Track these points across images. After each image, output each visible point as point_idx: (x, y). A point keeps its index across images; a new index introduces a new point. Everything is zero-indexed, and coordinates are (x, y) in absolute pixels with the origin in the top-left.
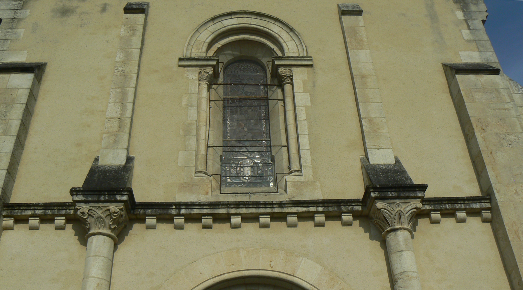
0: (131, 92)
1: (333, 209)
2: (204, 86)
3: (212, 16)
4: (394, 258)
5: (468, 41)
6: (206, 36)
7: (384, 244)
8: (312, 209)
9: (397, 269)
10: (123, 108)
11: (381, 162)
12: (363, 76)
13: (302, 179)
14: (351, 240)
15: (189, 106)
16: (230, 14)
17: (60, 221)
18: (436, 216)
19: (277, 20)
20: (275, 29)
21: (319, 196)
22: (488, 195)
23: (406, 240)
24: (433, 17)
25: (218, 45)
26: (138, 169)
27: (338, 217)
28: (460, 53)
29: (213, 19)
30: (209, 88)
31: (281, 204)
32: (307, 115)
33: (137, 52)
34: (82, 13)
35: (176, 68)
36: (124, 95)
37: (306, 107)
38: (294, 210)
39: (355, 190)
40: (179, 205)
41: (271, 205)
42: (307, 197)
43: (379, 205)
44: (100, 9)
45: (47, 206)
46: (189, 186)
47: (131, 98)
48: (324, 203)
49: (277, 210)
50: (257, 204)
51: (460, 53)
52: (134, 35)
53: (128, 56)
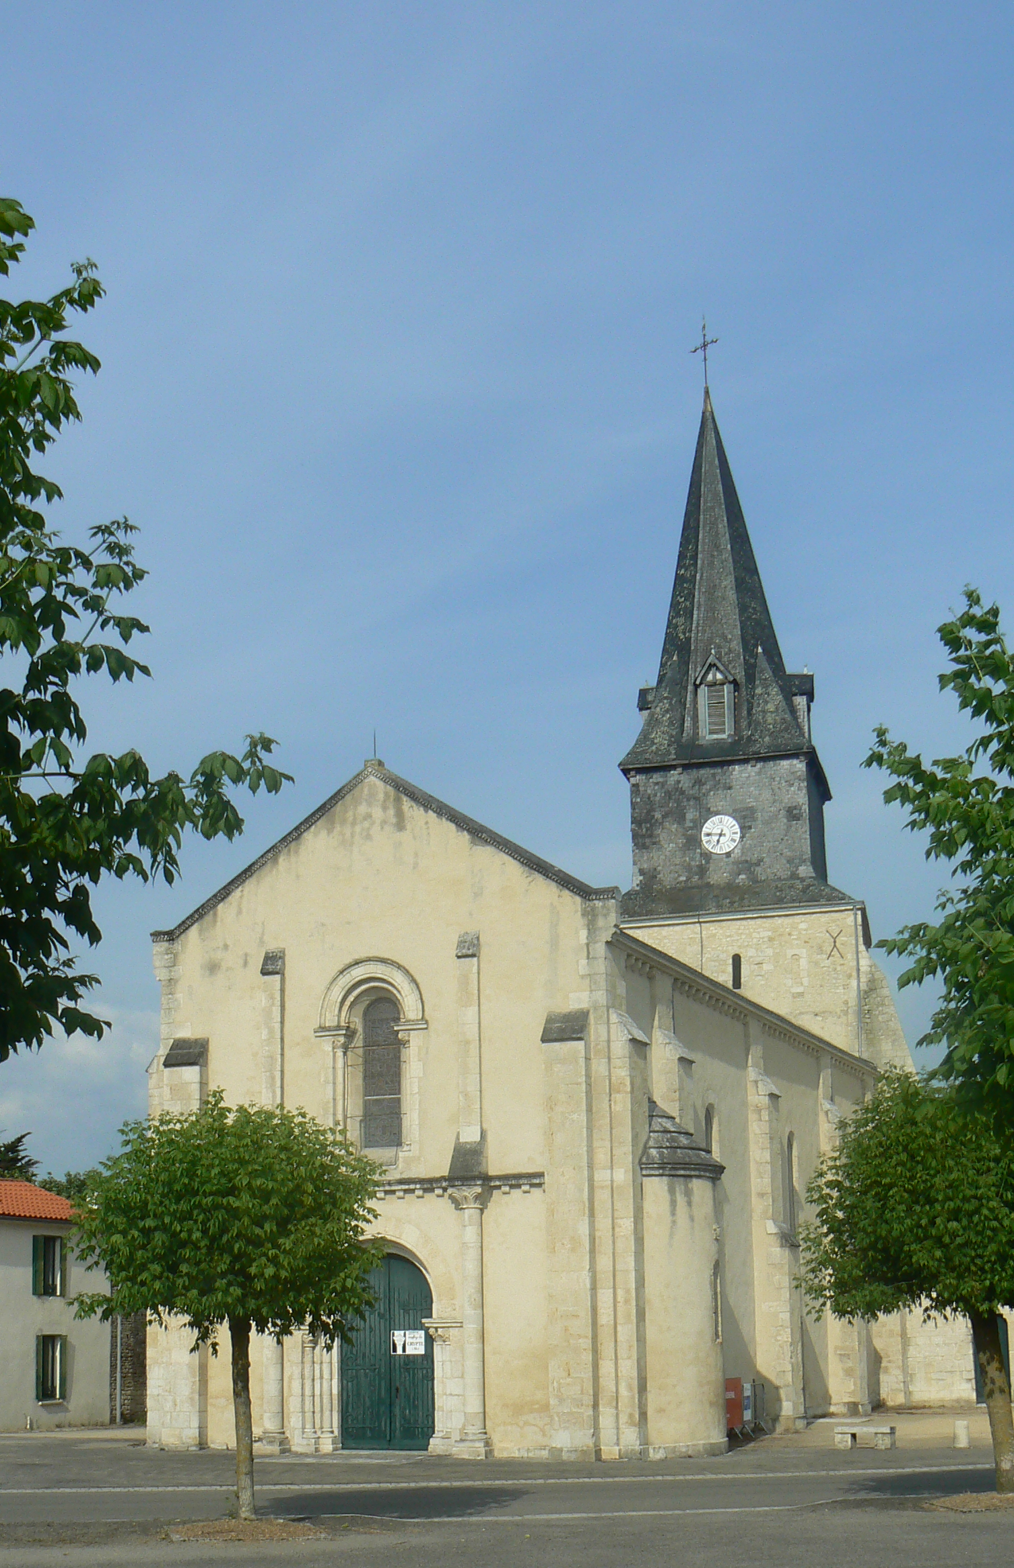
0: (278, 1075)
1: (428, 1185)
2: (340, 1053)
3: (341, 967)
5: (583, 977)
6: (337, 994)
8: (412, 1187)
10: (274, 1092)
11: (469, 1140)
12: (467, 1043)
13: (411, 1154)
15: (326, 1082)
16: (357, 963)
18: (507, 1189)
19: (399, 967)
20: (398, 978)
23: (470, 1217)
24: (554, 943)
25: (348, 1003)
28: (571, 995)
29: (342, 972)
30: (345, 1054)
31: (389, 1184)
32: (419, 1087)
33: (278, 1026)
35: (313, 1040)
36: (273, 1078)
37: (419, 1078)
38: (400, 1187)
44: (241, 962)
47: (278, 1084)
48: (421, 1181)
49: (387, 1188)
51: (571, 995)
52: (273, 1004)
53: (271, 1031)
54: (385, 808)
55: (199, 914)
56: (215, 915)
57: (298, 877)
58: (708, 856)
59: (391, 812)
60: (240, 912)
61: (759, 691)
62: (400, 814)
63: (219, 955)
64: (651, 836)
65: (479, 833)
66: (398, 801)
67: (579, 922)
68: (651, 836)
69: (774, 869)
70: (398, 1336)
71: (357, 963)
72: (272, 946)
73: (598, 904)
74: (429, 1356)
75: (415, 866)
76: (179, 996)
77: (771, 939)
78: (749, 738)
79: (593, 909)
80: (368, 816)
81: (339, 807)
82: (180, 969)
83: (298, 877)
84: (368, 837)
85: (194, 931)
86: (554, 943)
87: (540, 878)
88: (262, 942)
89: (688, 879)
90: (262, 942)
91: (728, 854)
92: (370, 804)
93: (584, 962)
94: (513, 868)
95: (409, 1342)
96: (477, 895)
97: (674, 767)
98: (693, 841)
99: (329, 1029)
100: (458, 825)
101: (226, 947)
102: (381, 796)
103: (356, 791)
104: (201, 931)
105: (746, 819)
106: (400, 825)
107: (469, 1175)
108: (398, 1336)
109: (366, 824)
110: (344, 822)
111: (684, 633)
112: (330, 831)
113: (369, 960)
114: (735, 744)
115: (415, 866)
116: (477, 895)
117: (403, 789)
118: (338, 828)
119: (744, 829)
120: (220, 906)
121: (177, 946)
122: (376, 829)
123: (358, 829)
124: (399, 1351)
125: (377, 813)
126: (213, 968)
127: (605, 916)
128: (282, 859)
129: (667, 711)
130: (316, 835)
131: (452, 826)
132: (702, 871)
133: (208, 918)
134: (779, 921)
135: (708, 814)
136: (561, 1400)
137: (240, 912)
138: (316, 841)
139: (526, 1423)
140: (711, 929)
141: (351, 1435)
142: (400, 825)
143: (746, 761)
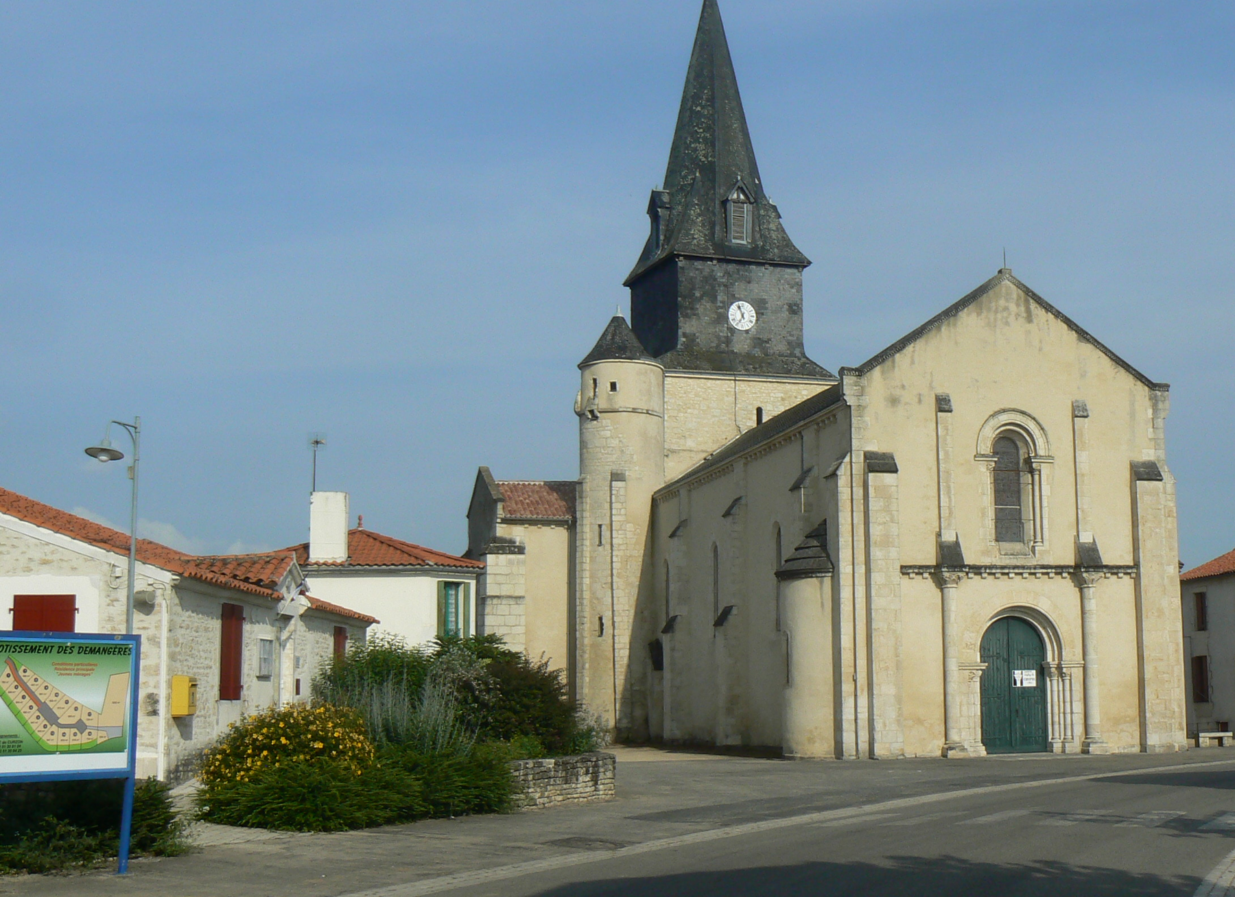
4: (1086, 602)
7: (1081, 590)
9: (1087, 608)
14: (1065, 585)
16: (1004, 411)
17: (926, 575)
20: (1031, 426)
21: (1052, 563)
22: (1137, 565)
24: (1132, 414)
26: (960, 540)
27: (1060, 574)
29: (992, 416)
34: (906, 404)
39: (1069, 559)
40: (986, 567)
41: (1029, 568)
42: (1045, 563)
43: (1085, 575)
45: (921, 567)
46: (986, 553)
50: (1023, 567)
54: (1018, 305)
55: (883, 357)
56: (893, 362)
57: (956, 343)
58: (732, 330)
59: (1023, 309)
60: (913, 362)
61: (762, 212)
62: (1028, 311)
63: (898, 392)
64: (692, 309)
65: (1083, 335)
66: (1027, 302)
67: (1148, 403)
68: (692, 309)
69: (778, 347)
70: (1017, 674)
71: (1004, 411)
72: (940, 391)
73: (1159, 393)
74: (1041, 688)
75: (1040, 350)
76: (867, 419)
77: (783, 399)
78: (763, 247)
79: (1156, 396)
80: (1006, 309)
81: (984, 298)
82: (866, 400)
83: (956, 343)
84: (1007, 323)
85: (877, 372)
86: (1132, 414)
87: (1122, 371)
88: (931, 387)
89: (718, 346)
90: (931, 387)
91: (747, 332)
92: (1007, 300)
93: (1151, 430)
94: (1106, 361)
95: (1026, 678)
96: (1083, 375)
97: (711, 259)
98: (723, 318)
99: (983, 456)
100: (1069, 326)
101: (903, 387)
102: (1015, 296)
103: (997, 289)
104: (883, 373)
105: (760, 307)
106: (1029, 319)
107: (1085, 565)
108: (1017, 674)
109: (1005, 314)
110: (989, 310)
111: (706, 157)
112: (979, 314)
113: (1014, 410)
114: (755, 248)
115: (1040, 350)
116: (1083, 375)
117: (1030, 295)
118: (984, 315)
119: (759, 314)
120: (897, 356)
121: (864, 381)
122: (1012, 319)
123: (999, 316)
124: (1019, 685)
125: (1013, 307)
126: (894, 401)
127: (1163, 402)
128: (939, 329)
129: (699, 215)
130: (968, 315)
131: (1065, 326)
132: (728, 341)
133: (888, 363)
134: (788, 387)
135: (733, 299)
136: (1153, 714)
137: (913, 362)
138: (968, 318)
139: (1122, 731)
140: (742, 386)
141: (988, 741)
142: (1029, 319)
143: (763, 264)
